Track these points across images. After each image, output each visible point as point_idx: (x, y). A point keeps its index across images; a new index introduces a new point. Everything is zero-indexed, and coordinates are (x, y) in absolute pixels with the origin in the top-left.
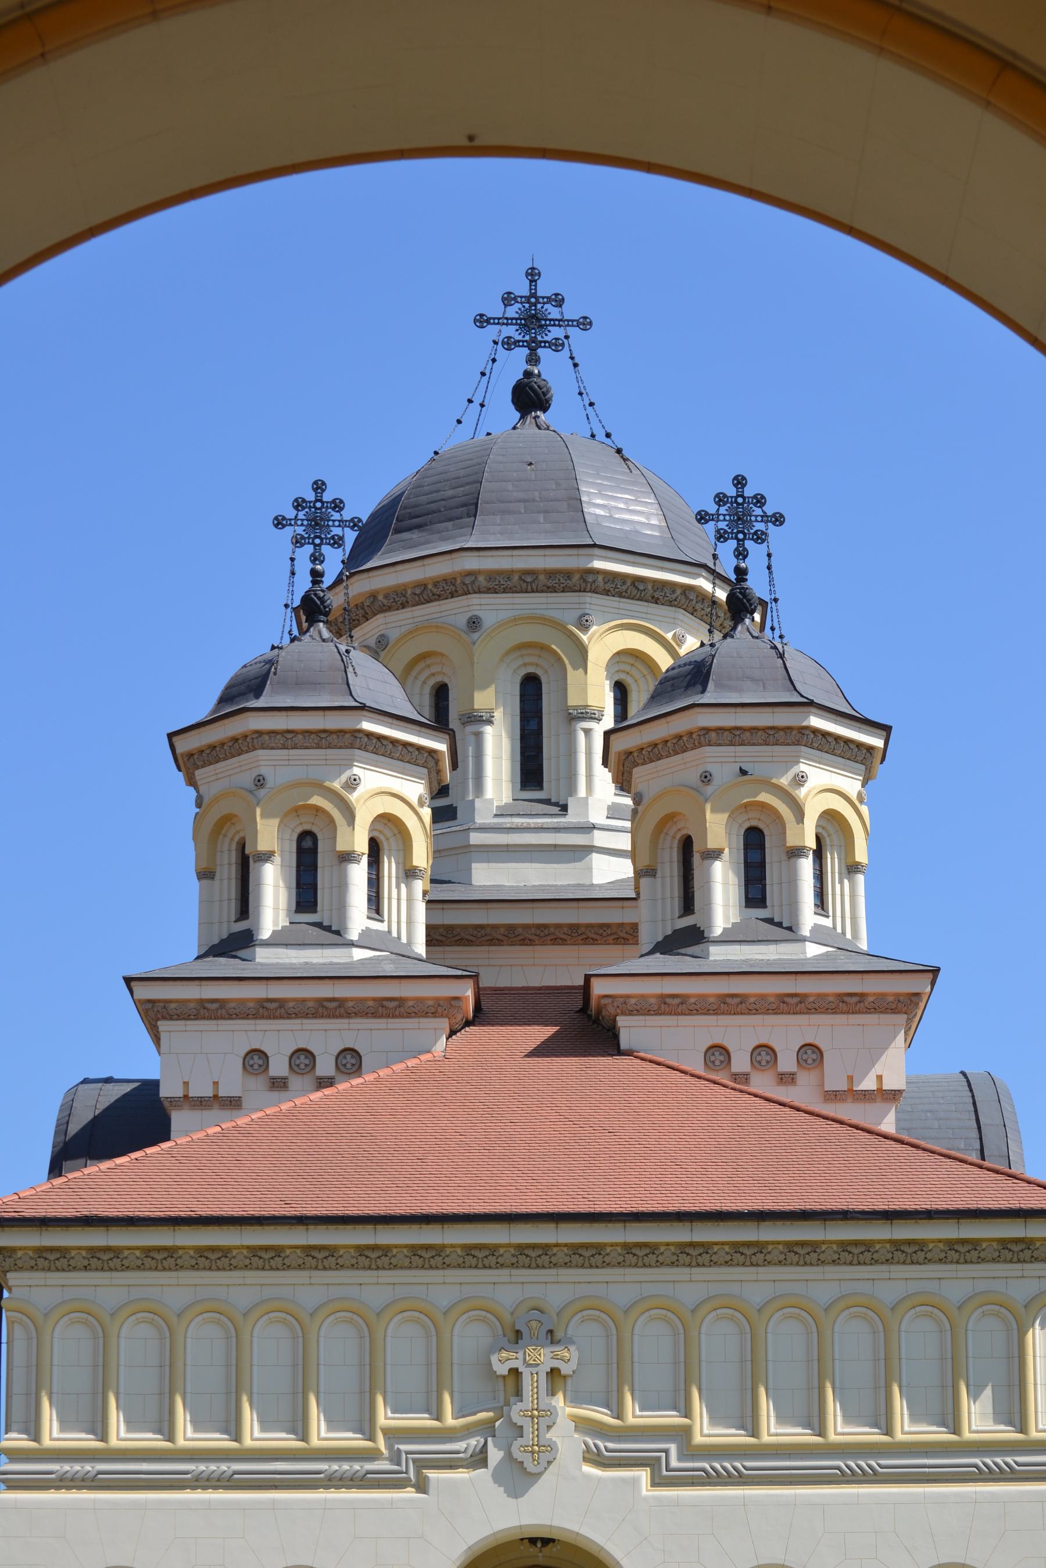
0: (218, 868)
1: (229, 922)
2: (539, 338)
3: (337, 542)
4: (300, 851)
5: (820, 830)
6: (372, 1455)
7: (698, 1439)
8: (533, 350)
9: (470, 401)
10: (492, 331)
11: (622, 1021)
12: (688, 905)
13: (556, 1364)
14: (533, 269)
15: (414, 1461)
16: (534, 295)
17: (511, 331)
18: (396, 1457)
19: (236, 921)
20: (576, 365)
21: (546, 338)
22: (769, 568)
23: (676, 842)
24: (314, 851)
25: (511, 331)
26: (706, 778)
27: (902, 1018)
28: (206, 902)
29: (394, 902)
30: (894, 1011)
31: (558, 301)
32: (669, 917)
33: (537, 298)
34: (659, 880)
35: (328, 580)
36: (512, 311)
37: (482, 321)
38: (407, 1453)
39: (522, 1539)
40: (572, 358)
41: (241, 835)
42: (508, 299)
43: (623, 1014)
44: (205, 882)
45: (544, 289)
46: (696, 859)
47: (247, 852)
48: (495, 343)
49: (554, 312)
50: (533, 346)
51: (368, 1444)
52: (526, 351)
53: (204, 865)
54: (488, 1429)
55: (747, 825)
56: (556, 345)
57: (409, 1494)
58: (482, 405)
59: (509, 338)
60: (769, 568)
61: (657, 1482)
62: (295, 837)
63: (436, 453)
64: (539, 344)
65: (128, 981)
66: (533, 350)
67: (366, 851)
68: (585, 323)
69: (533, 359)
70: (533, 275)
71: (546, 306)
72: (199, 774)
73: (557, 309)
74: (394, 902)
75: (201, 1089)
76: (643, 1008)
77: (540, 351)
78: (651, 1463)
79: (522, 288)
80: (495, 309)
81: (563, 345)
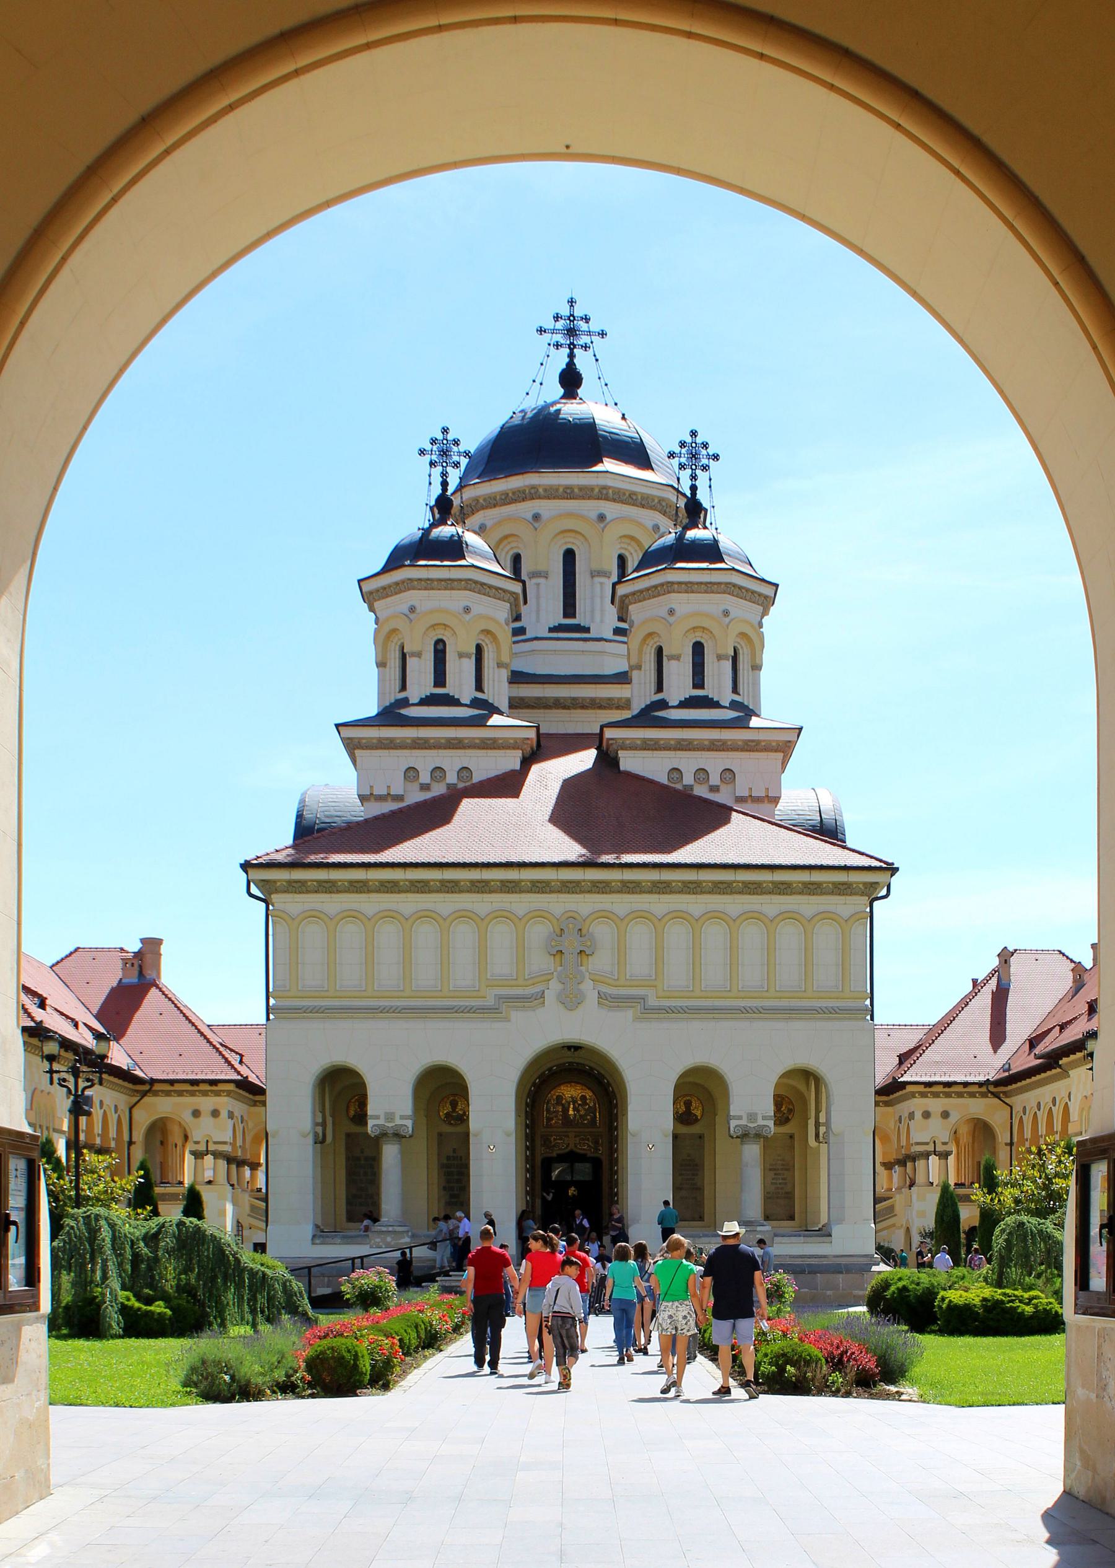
0: (388, 661)
1: (395, 692)
2: (575, 342)
3: (457, 465)
4: (436, 651)
5: (736, 645)
8: (572, 350)
9: (534, 381)
10: (547, 337)
11: (621, 753)
12: (660, 688)
16: (573, 316)
17: (559, 338)
19: (400, 691)
20: (597, 360)
21: (579, 343)
22: (710, 487)
23: (653, 650)
24: (444, 651)
25: (559, 338)
26: (671, 612)
27: (780, 755)
28: (381, 681)
29: (491, 682)
30: (776, 750)
32: (648, 694)
34: (643, 671)
35: (451, 489)
36: (560, 324)
37: (541, 331)
39: (563, 1047)
40: (595, 356)
41: (402, 641)
42: (557, 318)
43: (622, 749)
44: (380, 669)
45: (578, 313)
46: (665, 659)
47: (405, 651)
48: (549, 345)
49: (583, 326)
50: (572, 347)
52: (568, 351)
53: (380, 658)
55: (694, 641)
56: (585, 347)
58: (541, 384)
59: (557, 342)
60: (710, 487)
62: (433, 643)
63: (514, 413)
64: (575, 346)
65: (337, 726)
66: (572, 350)
67: (475, 652)
68: (603, 334)
69: (571, 356)
71: (581, 323)
72: (377, 604)
73: (586, 324)
74: (491, 682)
75: (380, 790)
76: (633, 746)
77: (575, 350)
79: (565, 311)
80: (549, 324)
81: (589, 348)
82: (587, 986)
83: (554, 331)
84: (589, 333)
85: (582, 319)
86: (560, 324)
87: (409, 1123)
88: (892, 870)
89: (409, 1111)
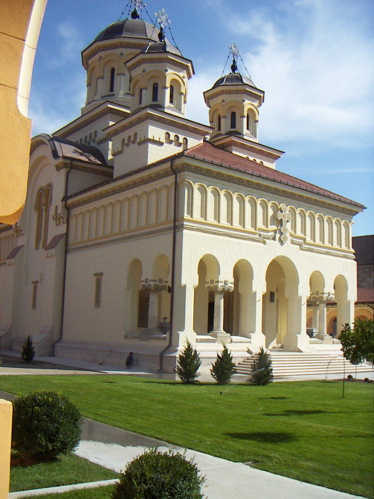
6: (255, 234)
7: (307, 241)
15: (263, 237)
18: (260, 235)
38: (262, 235)
51: (255, 231)
54: (275, 232)
57: (262, 244)
61: (301, 249)
75: (156, 139)
78: (300, 245)
87: (233, 286)
88: (363, 208)
89: (233, 281)
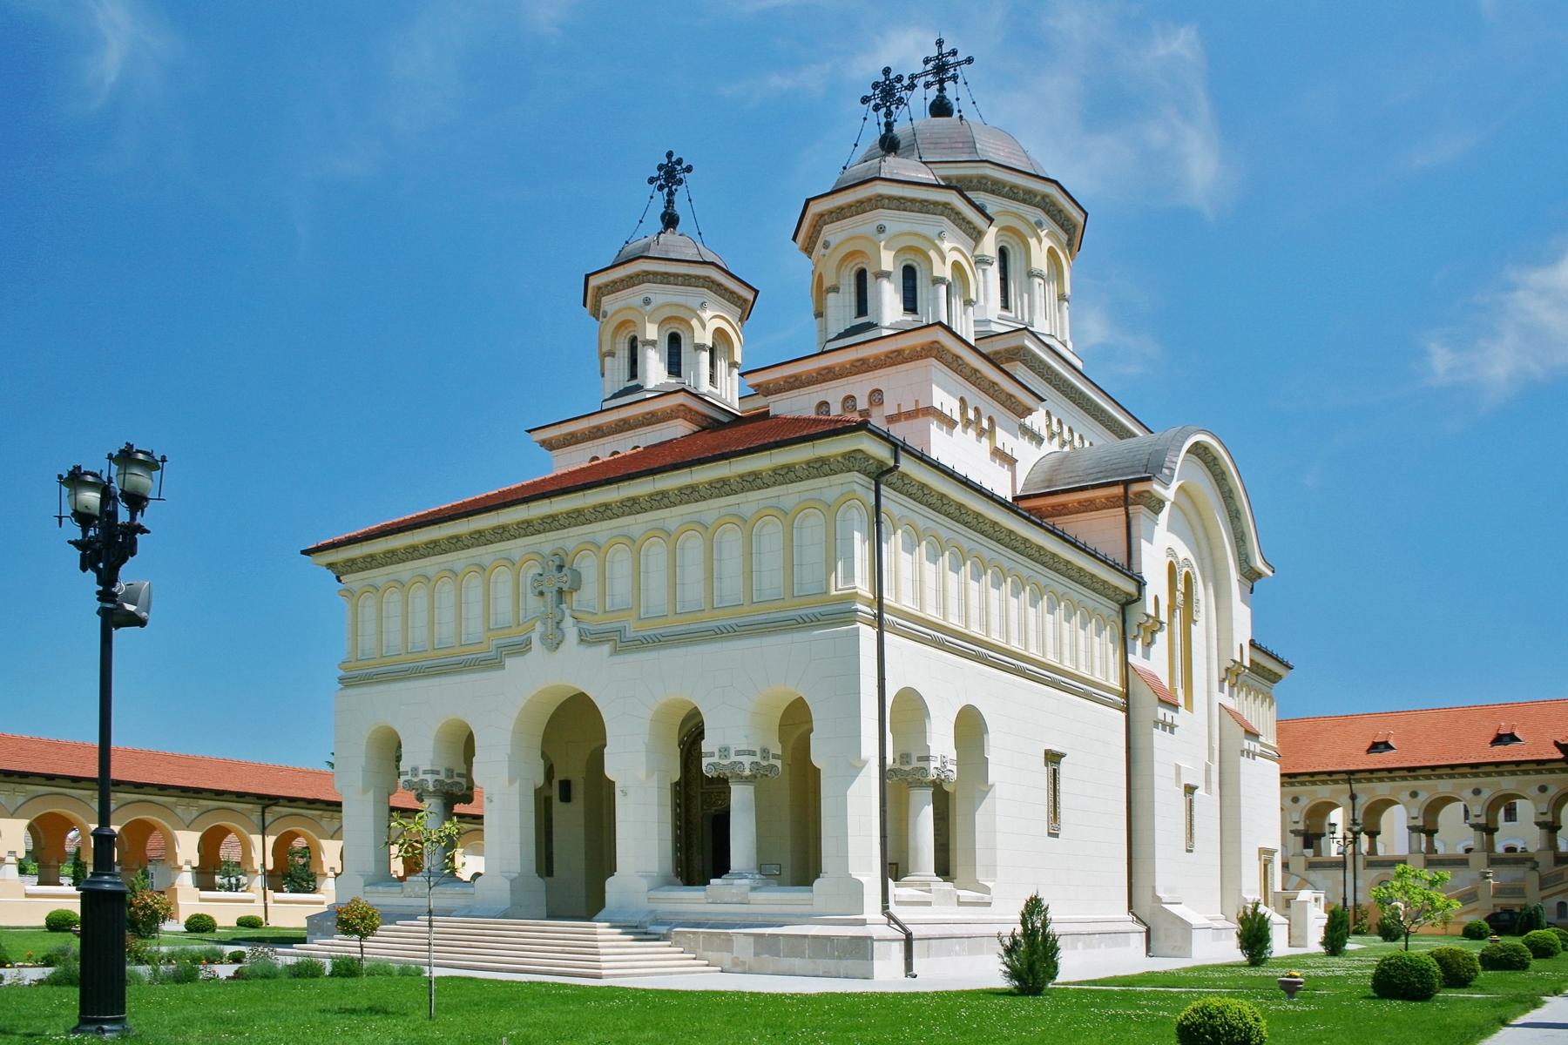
13: (561, 585)
14: (940, 40)
17: (930, 78)
31: (954, 53)
33: (943, 55)
36: (929, 67)
45: (945, 50)
49: (951, 60)
50: (941, 82)
56: (954, 78)
68: (969, 60)
70: (940, 43)
71: (949, 58)
82: (568, 622)
83: (926, 73)
84: (959, 64)
85: (949, 53)
86: (929, 67)
